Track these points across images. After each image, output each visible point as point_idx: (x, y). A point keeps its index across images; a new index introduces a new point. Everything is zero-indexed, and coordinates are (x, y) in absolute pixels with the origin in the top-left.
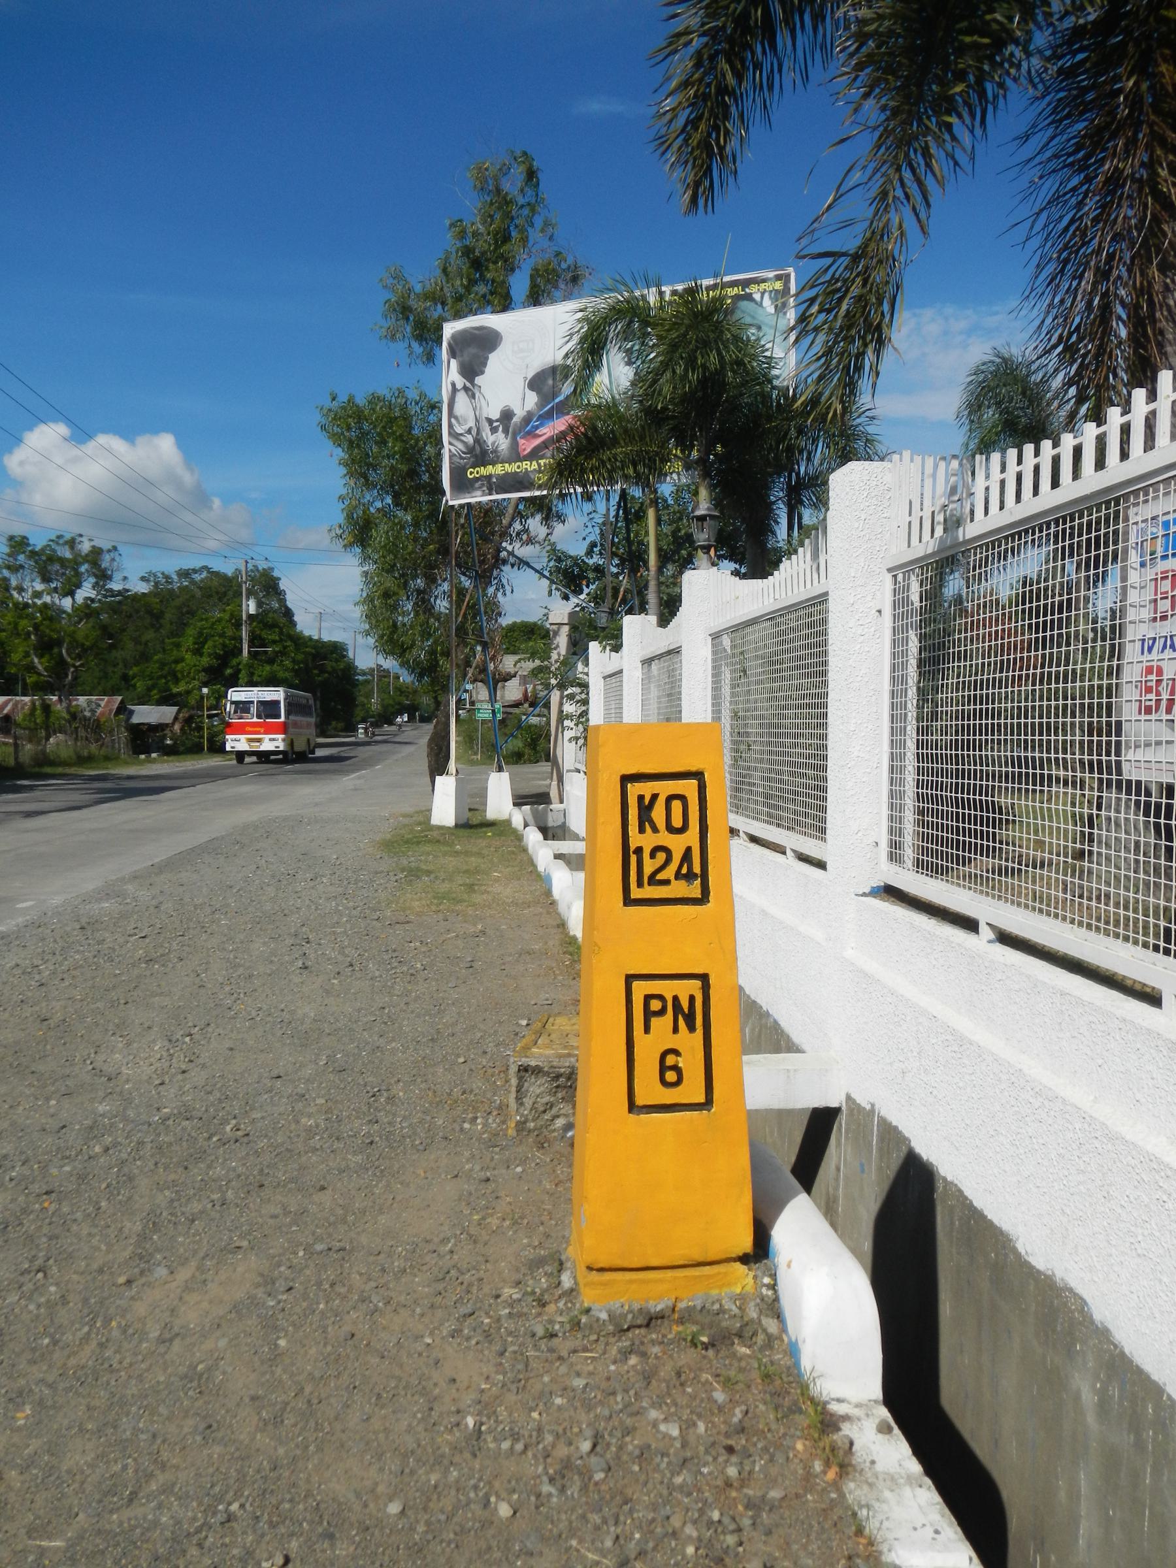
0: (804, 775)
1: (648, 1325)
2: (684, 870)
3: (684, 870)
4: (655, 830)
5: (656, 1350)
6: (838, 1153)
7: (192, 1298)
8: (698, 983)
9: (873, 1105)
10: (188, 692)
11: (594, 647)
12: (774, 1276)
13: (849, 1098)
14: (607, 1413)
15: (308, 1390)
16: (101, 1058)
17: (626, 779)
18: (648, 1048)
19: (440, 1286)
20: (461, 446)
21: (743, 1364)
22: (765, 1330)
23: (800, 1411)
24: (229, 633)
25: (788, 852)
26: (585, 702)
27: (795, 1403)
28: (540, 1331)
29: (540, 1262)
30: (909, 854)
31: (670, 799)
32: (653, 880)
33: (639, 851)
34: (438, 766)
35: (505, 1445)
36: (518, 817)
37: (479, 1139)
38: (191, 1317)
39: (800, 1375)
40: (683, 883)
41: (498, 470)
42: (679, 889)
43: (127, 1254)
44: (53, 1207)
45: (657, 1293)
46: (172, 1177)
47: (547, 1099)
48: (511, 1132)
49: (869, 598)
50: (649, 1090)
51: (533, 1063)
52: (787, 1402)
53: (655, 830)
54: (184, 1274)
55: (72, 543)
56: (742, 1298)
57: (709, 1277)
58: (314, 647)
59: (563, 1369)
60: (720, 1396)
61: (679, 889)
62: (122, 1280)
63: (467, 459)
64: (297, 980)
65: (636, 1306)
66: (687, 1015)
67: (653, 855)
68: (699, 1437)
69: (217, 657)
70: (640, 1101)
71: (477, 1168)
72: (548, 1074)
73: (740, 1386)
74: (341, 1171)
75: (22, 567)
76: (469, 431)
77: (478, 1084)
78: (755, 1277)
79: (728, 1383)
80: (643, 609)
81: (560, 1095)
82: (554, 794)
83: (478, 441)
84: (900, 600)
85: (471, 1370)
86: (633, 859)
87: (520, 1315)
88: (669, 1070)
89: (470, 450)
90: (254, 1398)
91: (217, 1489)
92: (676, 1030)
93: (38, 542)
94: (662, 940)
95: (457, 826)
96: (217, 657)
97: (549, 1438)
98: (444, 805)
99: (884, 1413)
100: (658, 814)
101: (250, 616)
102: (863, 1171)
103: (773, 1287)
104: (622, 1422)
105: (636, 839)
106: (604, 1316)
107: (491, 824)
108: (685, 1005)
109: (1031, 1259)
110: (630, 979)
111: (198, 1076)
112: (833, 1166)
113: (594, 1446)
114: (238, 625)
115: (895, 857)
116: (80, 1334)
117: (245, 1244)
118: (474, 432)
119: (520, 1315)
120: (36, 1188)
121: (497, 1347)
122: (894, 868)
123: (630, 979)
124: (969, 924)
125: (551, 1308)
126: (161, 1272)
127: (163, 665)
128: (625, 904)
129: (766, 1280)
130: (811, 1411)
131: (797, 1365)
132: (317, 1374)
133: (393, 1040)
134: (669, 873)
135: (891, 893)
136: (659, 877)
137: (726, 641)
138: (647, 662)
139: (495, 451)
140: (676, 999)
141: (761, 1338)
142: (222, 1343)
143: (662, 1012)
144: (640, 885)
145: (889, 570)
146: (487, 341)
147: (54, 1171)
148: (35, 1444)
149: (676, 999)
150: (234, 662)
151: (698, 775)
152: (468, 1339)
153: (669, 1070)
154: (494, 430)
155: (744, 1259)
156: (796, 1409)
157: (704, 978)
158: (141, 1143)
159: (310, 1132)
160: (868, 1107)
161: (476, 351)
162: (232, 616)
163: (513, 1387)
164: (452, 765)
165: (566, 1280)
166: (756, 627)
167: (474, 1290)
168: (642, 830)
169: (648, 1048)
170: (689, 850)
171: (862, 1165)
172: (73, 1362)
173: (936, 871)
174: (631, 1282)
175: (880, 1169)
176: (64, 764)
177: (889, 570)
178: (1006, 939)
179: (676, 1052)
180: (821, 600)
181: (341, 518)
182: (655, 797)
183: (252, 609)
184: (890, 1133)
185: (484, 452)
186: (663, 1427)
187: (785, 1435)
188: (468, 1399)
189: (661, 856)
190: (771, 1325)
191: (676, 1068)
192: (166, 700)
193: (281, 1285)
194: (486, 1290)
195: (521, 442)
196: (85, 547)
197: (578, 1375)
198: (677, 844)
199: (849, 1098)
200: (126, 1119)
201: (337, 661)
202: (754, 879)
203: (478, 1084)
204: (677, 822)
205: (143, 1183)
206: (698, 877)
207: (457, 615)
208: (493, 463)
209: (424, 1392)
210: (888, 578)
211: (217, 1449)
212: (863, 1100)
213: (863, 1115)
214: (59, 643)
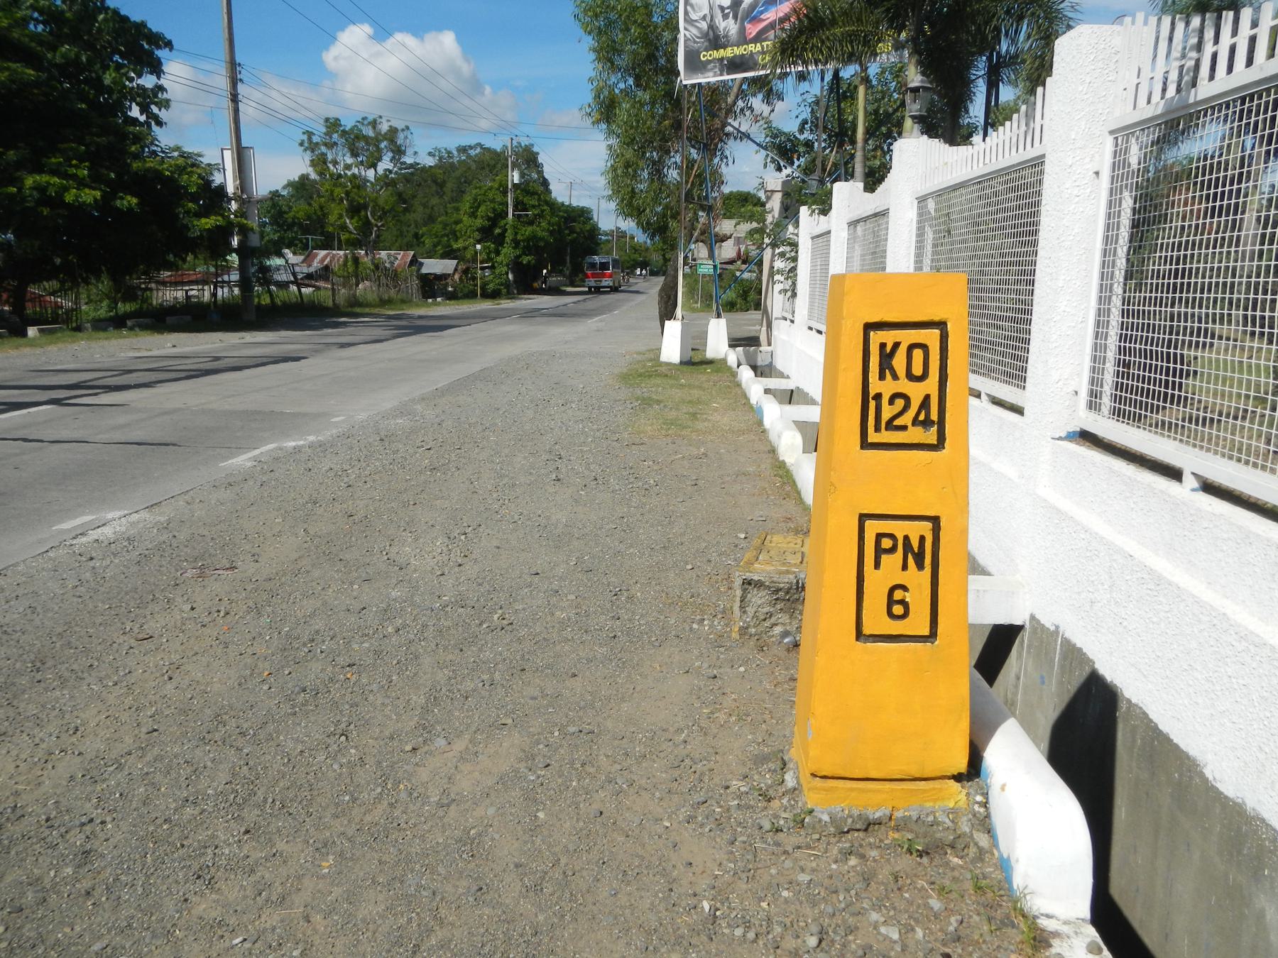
0: (998, 327)
1: (866, 830)
2: (922, 417)
3: (922, 417)
4: (895, 377)
5: (874, 853)
6: (1017, 662)
7: (465, 768)
8: (929, 525)
9: (1057, 627)
10: (465, 248)
11: (804, 211)
12: (986, 795)
13: (1033, 618)
14: (830, 910)
15: (563, 861)
16: (394, 550)
17: (869, 327)
18: (877, 583)
19: (676, 773)
20: (694, 31)
21: (956, 873)
22: (976, 844)
23: (1013, 926)
24: (499, 199)
25: (983, 396)
26: (795, 259)
27: (1008, 916)
28: (767, 826)
29: (764, 759)
30: (1106, 401)
31: (912, 347)
32: (890, 425)
33: (878, 397)
34: (667, 312)
35: (739, 932)
36: (732, 357)
37: (706, 639)
38: (464, 785)
39: (1010, 888)
40: (919, 429)
41: (728, 53)
42: (916, 435)
43: (412, 724)
44: (354, 679)
45: (877, 802)
46: (450, 657)
47: (766, 610)
48: (735, 635)
49: (1087, 160)
50: (877, 621)
51: (756, 578)
52: (999, 914)
53: (895, 377)
54: (459, 745)
55: (374, 124)
56: (954, 811)
57: (925, 791)
58: (566, 212)
59: (788, 864)
60: (935, 904)
61: (916, 435)
62: (408, 748)
63: (702, 43)
64: (551, 490)
65: (856, 813)
66: (915, 554)
67: (891, 402)
68: (917, 942)
69: (489, 219)
70: (867, 630)
71: (705, 665)
72: (769, 588)
73: (954, 895)
74: (589, 661)
75: (335, 144)
76: (704, 18)
77: (703, 588)
78: (968, 795)
79: (942, 891)
80: (849, 176)
81: (778, 607)
82: (763, 338)
83: (712, 27)
84: (1119, 160)
85: (705, 855)
86: (872, 404)
87: (749, 807)
88: (896, 603)
89: (705, 35)
90: (517, 866)
91: (487, 949)
92: (905, 567)
93: (348, 123)
94: (898, 482)
95: (681, 363)
96: (489, 219)
97: (778, 929)
98: (671, 346)
99: (1092, 933)
100: (899, 362)
101: (514, 185)
102: (1043, 683)
103: (985, 805)
104: (844, 921)
105: (875, 386)
106: (826, 818)
107: (710, 362)
108: (915, 544)
109: (1218, 785)
110: (863, 518)
111: (471, 570)
112: (1013, 675)
113: (820, 941)
114: (505, 193)
115: (1093, 405)
116: (374, 794)
117: (509, 721)
118: (708, 19)
119: (749, 807)
120: (341, 660)
121: (727, 836)
122: (1092, 415)
123: (863, 518)
124: (1174, 474)
125: (775, 804)
126: (441, 742)
127: (445, 225)
128: (862, 447)
129: (979, 798)
130: (1023, 926)
131: (1008, 880)
132: (571, 848)
133: (631, 546)
134: (907, 419)
135: (1087, 437)
136: (897, 423)
137: (931, 205)
138: (853, 224)
139: (726, 36)
140: (906, 538)
141: (972, 851)
142: (491, 811)
143: (892, 550)
144: (877, 429)
145: (1111, 132)
147: (356, 647)
148: (337, 891)
149: (906, 538)
150: (502, 223)
151: (941, 325)
152: (702, 825)
153: (896, 603)
154: (725, 17)
155: (958, 778)
156: (1007, 922)
157: (935, 520)
158: (425, 626)
159: (563, 625)
160: (1052, 628)
162: (501, 185)
163: (744, 876)
164: (679, 312)
165: (790, 780)
166: (963, 191)
167: (706, 779)
168: (882, 377)
169: (877, 583)
170: (927, 397)
171: (1042, 677)
172: (368, 818)
173: (1136, 419)
174: (852, 790)
175: (1060, 683)
176: (368, 305)
177: (1111, 132)
178: (1210, 488)
179: (904, 588)
180: (1037, 163)
181: (589, 98)
182: (896, 345)
183: (516, 181)
184: (1073, 654)
185: (717, 37)
186: (883, 930)
187: (999, 947)
188: (703, 883)
189: (900, 403)
190: (983, 839)
191: (902, 602)
192: (449, 254)
193: (540, 762)
194: (717, 780)
195: (748, 26)
196: (384, 127)
197: (803, 870)
198: (916, 392)
199: (1033, 618)
200: (413, 604)
201: (584, 223)
202: (979, 425)
203: (703, 588)
204: (917, 370)
205: (427, 661)
206: (936, 424)
207: (687, 182)
208: (725, 47)
209: (664, 873)
210: (1109, 141)
211: (487, 911)
212: (1047, 621)
213: (1046, 637)
214: (365, 207)
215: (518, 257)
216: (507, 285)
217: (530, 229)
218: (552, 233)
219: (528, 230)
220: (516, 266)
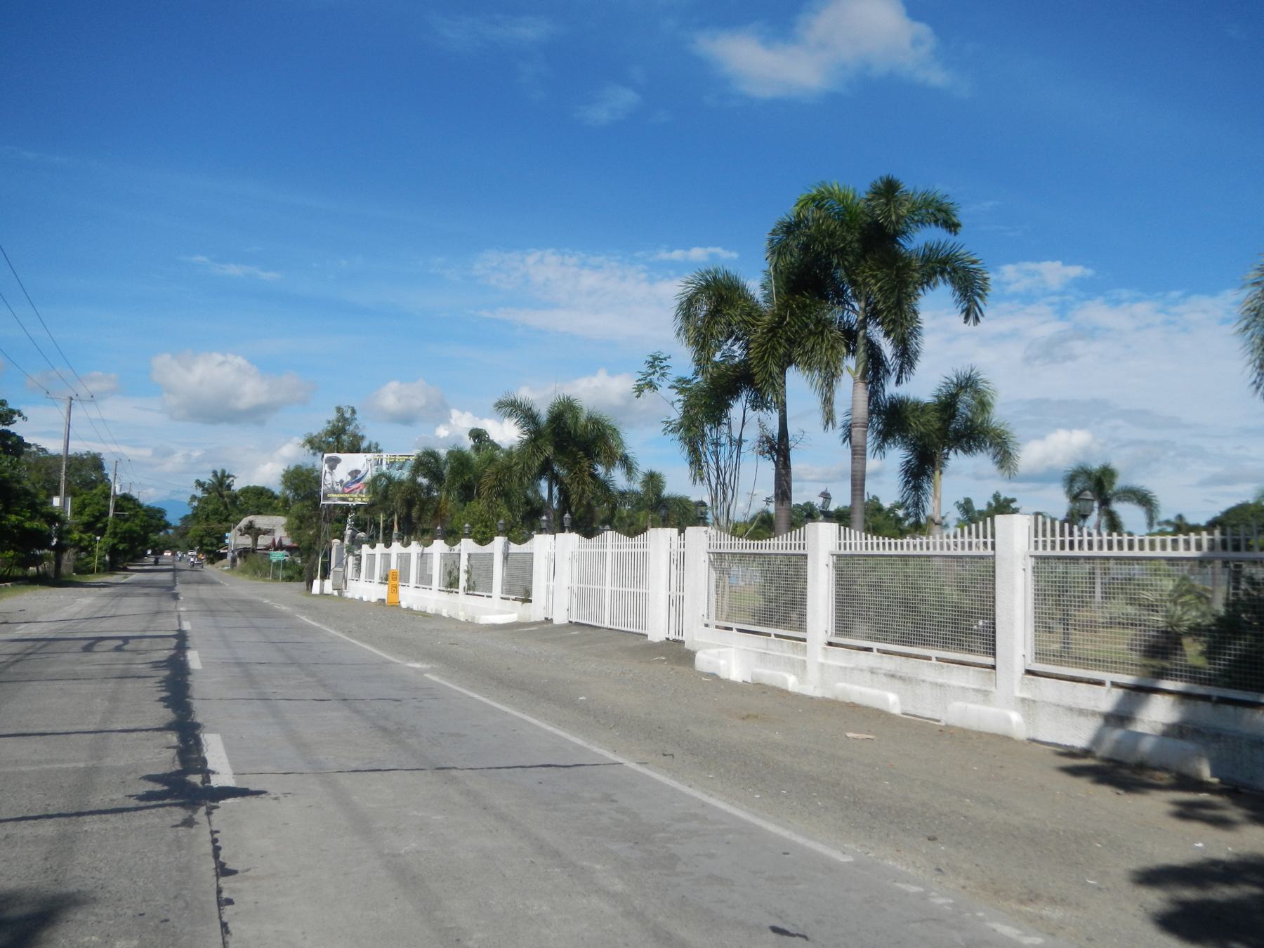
24: (103, 502)
96: (94, 516)
114: (107, 497)
146: (337, 461)
161: (334, 463)
215: (114, 545)
216: (104, 564)
217: (128, 524)
218: (142, 527)
219: (126, 526)
220: (113, 551)
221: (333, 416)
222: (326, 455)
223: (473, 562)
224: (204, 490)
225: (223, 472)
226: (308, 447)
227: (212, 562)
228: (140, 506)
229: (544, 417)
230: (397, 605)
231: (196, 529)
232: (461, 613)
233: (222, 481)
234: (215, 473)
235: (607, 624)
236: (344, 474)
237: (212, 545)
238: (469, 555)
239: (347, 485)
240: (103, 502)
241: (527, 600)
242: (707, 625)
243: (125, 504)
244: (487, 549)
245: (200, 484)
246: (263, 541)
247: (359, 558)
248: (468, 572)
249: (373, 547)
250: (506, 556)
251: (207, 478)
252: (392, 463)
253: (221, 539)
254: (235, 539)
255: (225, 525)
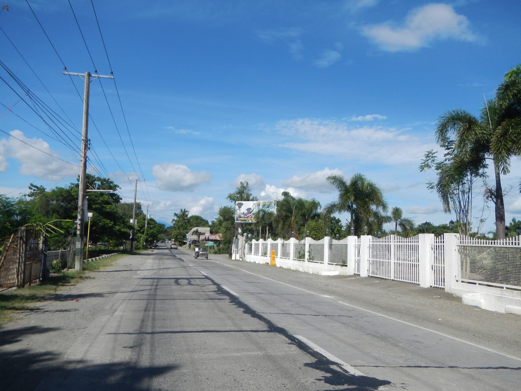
114: (145, 219)
146: (242, 204)
161: (240, 205)
215: (147, 239)
216: (143, 246)
218: (158, 232)
219: (151, 231)
220: (146, 241)
221: (239, 186)
222: (237, 202)
223: (312, 247)
224: (178, 217)
225: (185, 210)
226: (229, 199)
227: (181, 246)
228: (156, 223)
229: (348, 183)
230: (274, 266)
231: (174, 233)
232: (310, 270)
233: (184, 214)
234: (181, 210)
235: (392, 278)
236: (245, 210)
237: (181, 239)
238: (310, 245)
239: (246, 215)
240: (143, 222)
241: (344, 264)
242: (457, 281)
243: (151, 222)
244: (320, 242)
245: (176, 215)
246: (202, 237)
247: (251, 245)
248: (309, 252)
249: (257, 240)
250: (331, 246)
251: (178, 212)
252: (264, 205)
253: (184, 237)
254: (190, 237)
255: (186, 231)
